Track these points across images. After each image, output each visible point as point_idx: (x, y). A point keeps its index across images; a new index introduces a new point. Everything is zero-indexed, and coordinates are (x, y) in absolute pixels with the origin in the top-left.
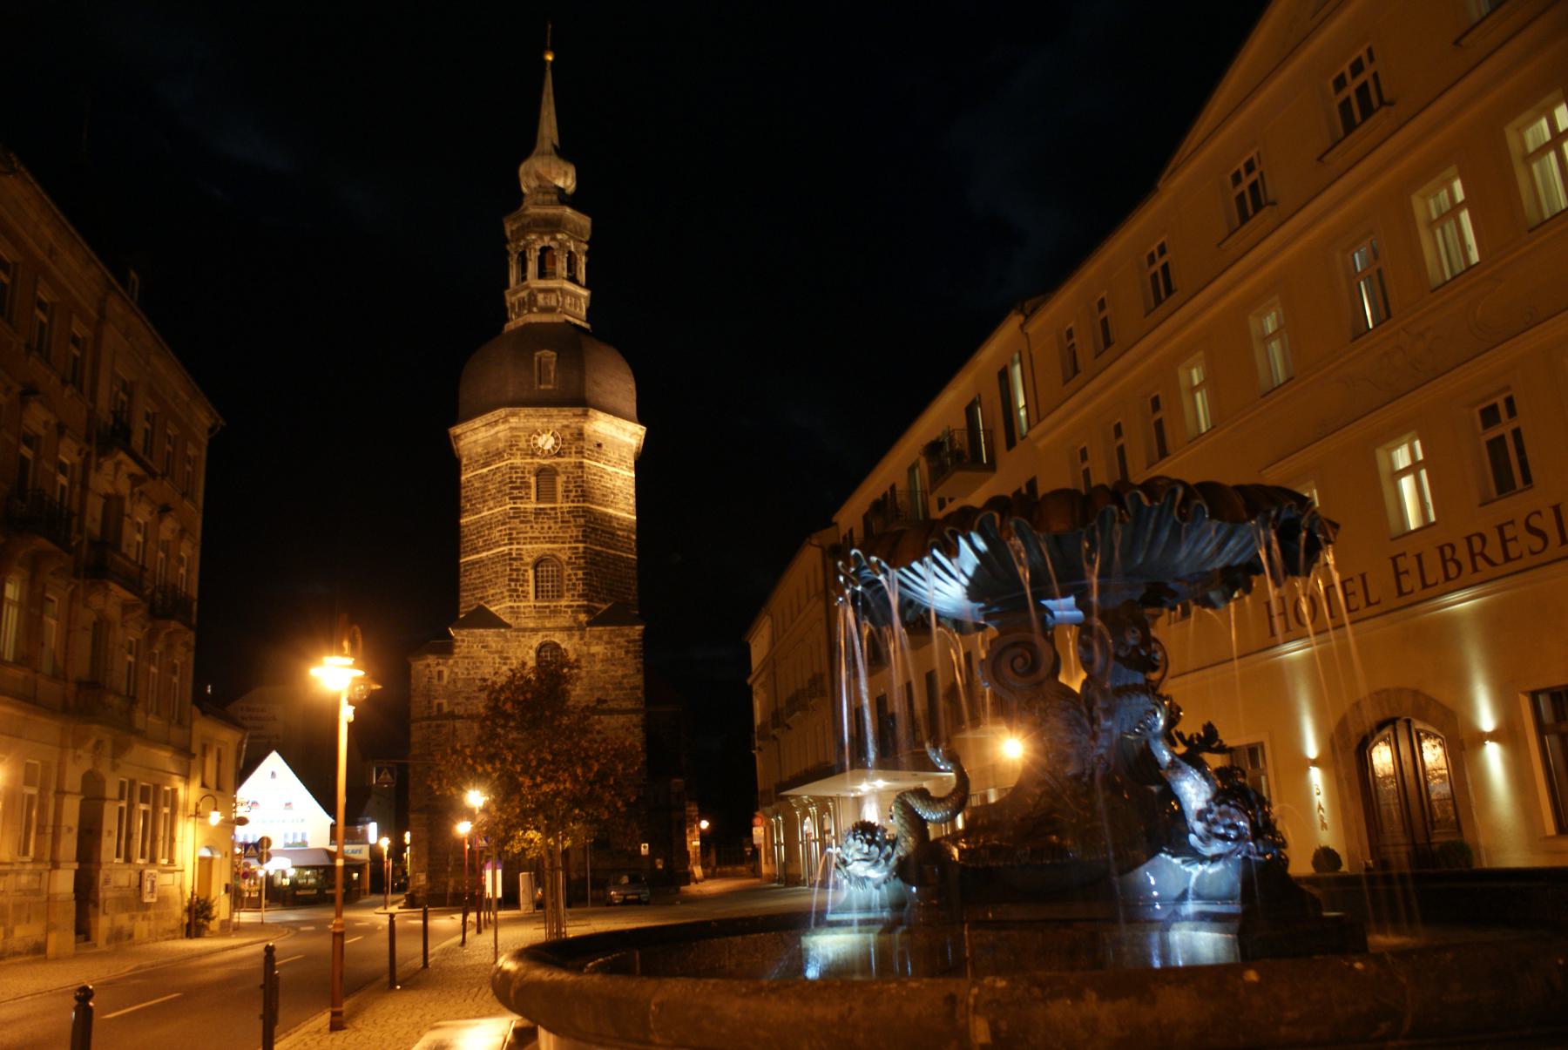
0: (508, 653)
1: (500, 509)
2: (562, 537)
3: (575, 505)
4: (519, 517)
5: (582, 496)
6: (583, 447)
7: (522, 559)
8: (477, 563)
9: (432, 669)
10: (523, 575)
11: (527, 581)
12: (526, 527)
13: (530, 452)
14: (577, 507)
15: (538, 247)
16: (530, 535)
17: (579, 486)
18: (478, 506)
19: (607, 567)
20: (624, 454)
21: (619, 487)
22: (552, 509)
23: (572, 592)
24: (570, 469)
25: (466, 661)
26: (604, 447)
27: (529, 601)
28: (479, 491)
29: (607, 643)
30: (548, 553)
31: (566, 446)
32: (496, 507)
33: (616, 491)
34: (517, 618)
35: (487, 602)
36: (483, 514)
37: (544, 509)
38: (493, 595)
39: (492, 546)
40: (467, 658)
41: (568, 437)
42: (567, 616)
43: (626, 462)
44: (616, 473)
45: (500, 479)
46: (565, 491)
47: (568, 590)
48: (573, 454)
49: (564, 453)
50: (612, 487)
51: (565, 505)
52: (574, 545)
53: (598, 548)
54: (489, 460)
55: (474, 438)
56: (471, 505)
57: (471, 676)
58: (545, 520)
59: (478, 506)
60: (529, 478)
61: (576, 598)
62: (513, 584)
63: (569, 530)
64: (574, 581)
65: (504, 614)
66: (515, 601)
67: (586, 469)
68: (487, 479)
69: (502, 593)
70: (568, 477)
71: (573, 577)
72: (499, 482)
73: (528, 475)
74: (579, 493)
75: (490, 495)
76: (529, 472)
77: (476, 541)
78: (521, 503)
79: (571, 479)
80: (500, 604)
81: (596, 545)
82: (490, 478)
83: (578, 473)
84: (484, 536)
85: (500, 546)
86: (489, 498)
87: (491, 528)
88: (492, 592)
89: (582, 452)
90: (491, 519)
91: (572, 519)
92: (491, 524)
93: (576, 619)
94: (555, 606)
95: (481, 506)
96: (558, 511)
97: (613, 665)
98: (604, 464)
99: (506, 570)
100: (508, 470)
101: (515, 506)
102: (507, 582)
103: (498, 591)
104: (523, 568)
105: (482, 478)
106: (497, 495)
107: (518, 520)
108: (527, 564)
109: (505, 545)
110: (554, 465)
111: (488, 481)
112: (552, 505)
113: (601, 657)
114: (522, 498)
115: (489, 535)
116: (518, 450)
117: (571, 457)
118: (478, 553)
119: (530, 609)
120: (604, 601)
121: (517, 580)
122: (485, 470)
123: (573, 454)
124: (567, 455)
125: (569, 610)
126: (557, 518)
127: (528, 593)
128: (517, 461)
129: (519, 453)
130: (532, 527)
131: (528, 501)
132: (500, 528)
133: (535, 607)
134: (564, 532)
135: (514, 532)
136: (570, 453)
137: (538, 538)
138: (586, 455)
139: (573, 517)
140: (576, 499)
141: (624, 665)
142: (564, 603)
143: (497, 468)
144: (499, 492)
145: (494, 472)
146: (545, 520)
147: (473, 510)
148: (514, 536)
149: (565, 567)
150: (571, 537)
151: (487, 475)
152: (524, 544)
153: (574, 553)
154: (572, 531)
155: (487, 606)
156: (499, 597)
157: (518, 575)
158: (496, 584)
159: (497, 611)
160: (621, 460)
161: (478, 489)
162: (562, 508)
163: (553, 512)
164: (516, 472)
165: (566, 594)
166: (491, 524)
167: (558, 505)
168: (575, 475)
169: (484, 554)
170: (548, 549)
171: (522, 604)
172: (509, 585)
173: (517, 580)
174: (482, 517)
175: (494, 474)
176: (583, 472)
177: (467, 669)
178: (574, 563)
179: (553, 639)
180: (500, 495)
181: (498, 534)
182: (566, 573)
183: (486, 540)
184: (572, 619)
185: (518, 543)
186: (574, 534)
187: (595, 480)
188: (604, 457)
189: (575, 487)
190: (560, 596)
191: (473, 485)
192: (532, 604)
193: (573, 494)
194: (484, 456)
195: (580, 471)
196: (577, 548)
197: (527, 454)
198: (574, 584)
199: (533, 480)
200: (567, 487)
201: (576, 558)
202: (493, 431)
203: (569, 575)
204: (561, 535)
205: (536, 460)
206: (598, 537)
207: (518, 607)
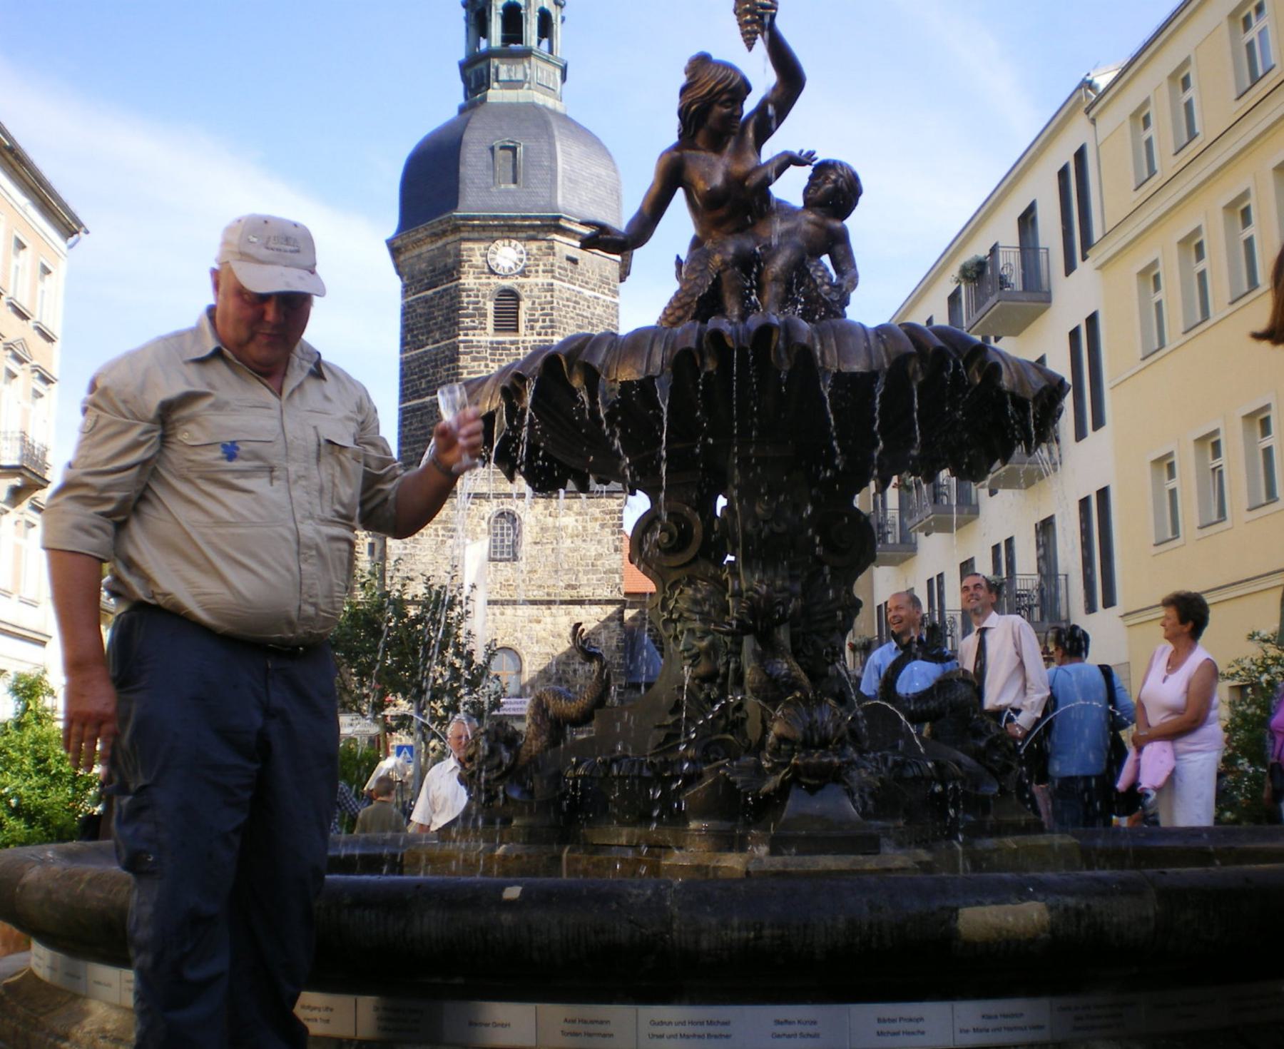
1: (447, 342)
3: (542, 337)
4: (472, 352)
5: (552, 327)
6: (552, 265)
8: (419, 409)
12: (479, 365)
17: (547, 315)
18: (420, 337)
20: (607, 274)
21: (599, 315)
22: (512, 343)
24: (536, 292)
28: (422, 320)
29: (580, 514)
31: (532, 262)
32: (442, 339)
33: (594, 321)
36: (428, 348)
37: (504, 343)
41: (535, 251)
43: (609, 284)
44: (597, 298)
45: (448, 304)
46: (530, 321)
49: (530, 271)
50: (589, 316)
51: (529, 338)
54: (435, 279)
55: (416, 252)
56: (412, 337)
57: (407, 551)
58: (504, 357)
59: (420, 337)
60: (485, 304)
68: (432, 304)
70: (534, 303)
72: (447, 308)
73: (482, 300)
74: (548, 323)
75: (436, 324)
76: (484, 296)
77: (418, 382)
79: (537, 305)
82: (435, 302)
84: (428, 375)
86: (435, 327)
87: (436, 366)
89: (552, 271)
90: (437, 354)
92: (436, 360)
95: (424, 338)
96: (520, 345)
97: (584, 541)
98: (580, 286)
105: (426, 302)
106: (444, 324)
107: (468, 357)
110: (516, 287)
111: (434, 306)
113: (570, 531)
114: (474, 328)
115: (434, 374)
116: (471, 267)
118: (420, 397)
122: (430, 292)
124: (533, 274)
129: (471, 270)
130: (487, 366)
131: (482, 332)
132: (448, 366)
136: (537, 272)
140: (543, 331)
141: (599, 542)
143: (445, 290)
144: (447, 319)
145: (441, 295)
146: (504, 357)
147: (414, 342)
151: (432, 299)
162: (523, 342)
163: (513, 347)
164: (469, 296)
166: (436, 360)
167: (521, 338)
168: (543, 300)
174: (425, 352)
175: (442, 297)
176: (552, 296)
179: (509, 507)
180: (448, 324)
183: (429, 382)
187: (568, 306)
189: (542, 315)
191: (415, 311)
193: (540, 324)
194: (429, 275)
195: (549, 294)
197: (483, 273)
199: (490, 307)
200: (531, 315)
202: (440, 243)
205: (494, 279)
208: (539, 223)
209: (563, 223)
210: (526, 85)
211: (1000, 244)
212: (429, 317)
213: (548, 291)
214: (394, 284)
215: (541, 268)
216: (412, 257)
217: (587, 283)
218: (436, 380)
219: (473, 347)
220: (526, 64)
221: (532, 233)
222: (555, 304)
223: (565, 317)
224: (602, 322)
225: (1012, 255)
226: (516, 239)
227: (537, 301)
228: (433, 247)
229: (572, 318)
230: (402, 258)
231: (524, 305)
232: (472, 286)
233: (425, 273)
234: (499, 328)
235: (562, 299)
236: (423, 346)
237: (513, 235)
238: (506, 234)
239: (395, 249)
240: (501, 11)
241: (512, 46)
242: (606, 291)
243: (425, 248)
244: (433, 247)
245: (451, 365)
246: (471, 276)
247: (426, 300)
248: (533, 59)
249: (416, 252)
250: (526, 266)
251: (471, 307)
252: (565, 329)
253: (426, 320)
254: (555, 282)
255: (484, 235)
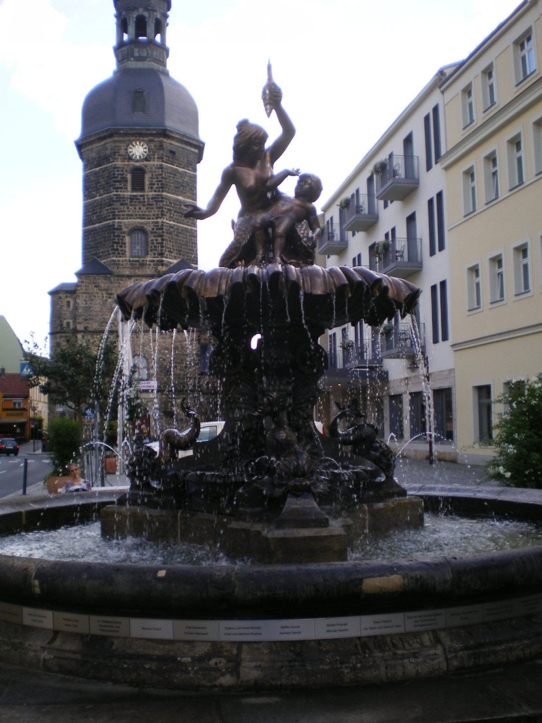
0: (111, 290)
2: (147, 215)
4: (120, 201)
5: (162, 188)
7: (121, 229)
9: (62, 300)
10: (122, 240)
11: (125, 244)
12: (124, 208)
13: (127, 157)
14: (158, 195)
15: (135, 16)
16: (127, 213)
18: (93, 193)
19: (177, 235)
20: (191, 160)
23: (154, 252)
24: (154, 169)
25: (85, 295)
26: (177, 154)
27: (125, 257)
30: (139, 225)
31: (151, 153)
32: (104, 194)
33: (184, 185)
34: (118, 268)
35: (99, 257)
38: (102, 253)
39: (102, 220)
40: (85, 293)
41: (153, 147)
42: (151, 267)
44: (186, 172)
45: (107, 175)
46: (150, 184)
47: (151, 250)
48: (156, 159)
49: (150, 158)
50: (181, 181)
51: (150, 193)
52: (155, 220)
53: (172, 223)
57: (88, 305)
58: (137, 203)
59: (93, 193)
61: (156, 256)
62: (115, 245)
63: (153, 211)
64: (155, 244)
65: (109, 265)
66: (116, 257)
67: (165, 170)
69: (108, 251)
70: (152, 175)
71: (155, 242)
72: (107, 177)
73: (125, 173)
74: (160, 186)
75: (101, 185)
76: (126, 171)
78: (121, 192)
80: (107, 258)
81: (170, 221)
82: (101, 174)
83: (159, 172)
84: (96, 213)
85: (107, 220)
86: (100, 187)
87: (101, 208)
88: (102, 250)
90: (101, 202)
91: (154, 203)
92: (101, 205)
93: (156, 270)
94: (143, 261)
95: (95, 193)
96: (145, 197)
99: (110, 236)
100: (112, 169)
101: (117, 193)
102: (111, 244)
103: (106, 250)
104: (123, 235)
107: (118, 204)
108: (124, 233)
109: (110, 219)
110: (143, 166)
112: (141, 193)
115: (100, 212)
116: (119, 155)
117: (154, 161)
118: (93, 224)
119: (126, 262)
120: (175, 258)
121: (118, 243)
122: (98, 169)
123: (156, 159)
124: (152, 160)
125: (152, 264)
126: (145, 202)
127: (125, 252)
128: (119, 163)
129: (120, 157)
130: (128, 208)
132: (107, 208)
133: (130, 261)
134: (149, 212)
135: (117, 211)
136: (154, 158)
137: (132, 215)
138: (165, 160)
139: (155, 201)
140: (157, 190)
142: (149, 258)
145: (104, 170)
146: (137, 203)
148: (116, 213)
149: (150, 235)
150: (154, 215)
151: (99, 172)
152: (123, 219)
153: (155, 226)
154: (154, 211)
155: (99, 260)
156: (107, 253)
157: (118, 240)
158: (104, 245)
159: (105, 263)
160: (188, 164)
161: (93, 181)
163: (142, 198)
164: (118, 171)
165: (150, 253)
166: (101, 205)
167: (146, 194)
168: (157, 173)
169: (97, 225)
170: (139, 223)
171: (121, 259)
172: (113, 246)
173: (118, 243)
174: (95, 200)
175: (104, 172)
176: (162, 171)
177: (85, 301)
178: (156, 233)
180: (107, 186)
181: (106, 212)
182: (150, 239)
183: (98, 216)
184: (154, 269)
185: (119, 218)
186: (156, 213)
187: (170, 177)
188: (177, 162)
189: (157, 181)
190: (147, 254)
191: (89, 179)
192: (128, 259)
193: (156, 186)
195: (160, 170)
196: (157, 222)
197: (125, 159)
198: (155, 247)
199: (129, 176)
200: (151, 181)
201: (157, 229)
202: (103, 143)
203: (152, 240)
204: (147, 213)
205: (132, 163)
206: (172, 215)
207: (119, 261)
208: (155, 132)
209: (167, 133)
210: (148, 59)
211: (394, 154)
212: (97, 182)
213: (160, 168)
214: (79, 164)
215: (156, 156)
216: (88, 150)
217: (180, 164)
218: (101, 215)
219: (120, 198)
220: (148, 48)
221: (151, 138)
222: (163, 176)
223: (169, 182)
224: (188, 185)
225: (400, 159)
226: (143, 141)
227: (154, 174)
228: (99, 145)
229: (172, 183)
230: (83, 150)
231: (147, 177)
232: (120, 166)
233: (95, 159)
234: (134, 190)
235: (167, 173)
236: (94, 197)
237: (142, 139)
238: (137, 138)
239: (80, 146)
240: (135, 20)
241: (140, 38)
242: (190, 169)
243: (94, 146)
244: (99, 145)
245: (109, 208)
246: (119, 160)
247: (96, 173)
248: (152, 46)
249: (90, 147)
250: (148, 155)
251: (119, 176)
252: (169, 189)
253: (96, 183)
254: (164, 164)
255: (126, 139)
